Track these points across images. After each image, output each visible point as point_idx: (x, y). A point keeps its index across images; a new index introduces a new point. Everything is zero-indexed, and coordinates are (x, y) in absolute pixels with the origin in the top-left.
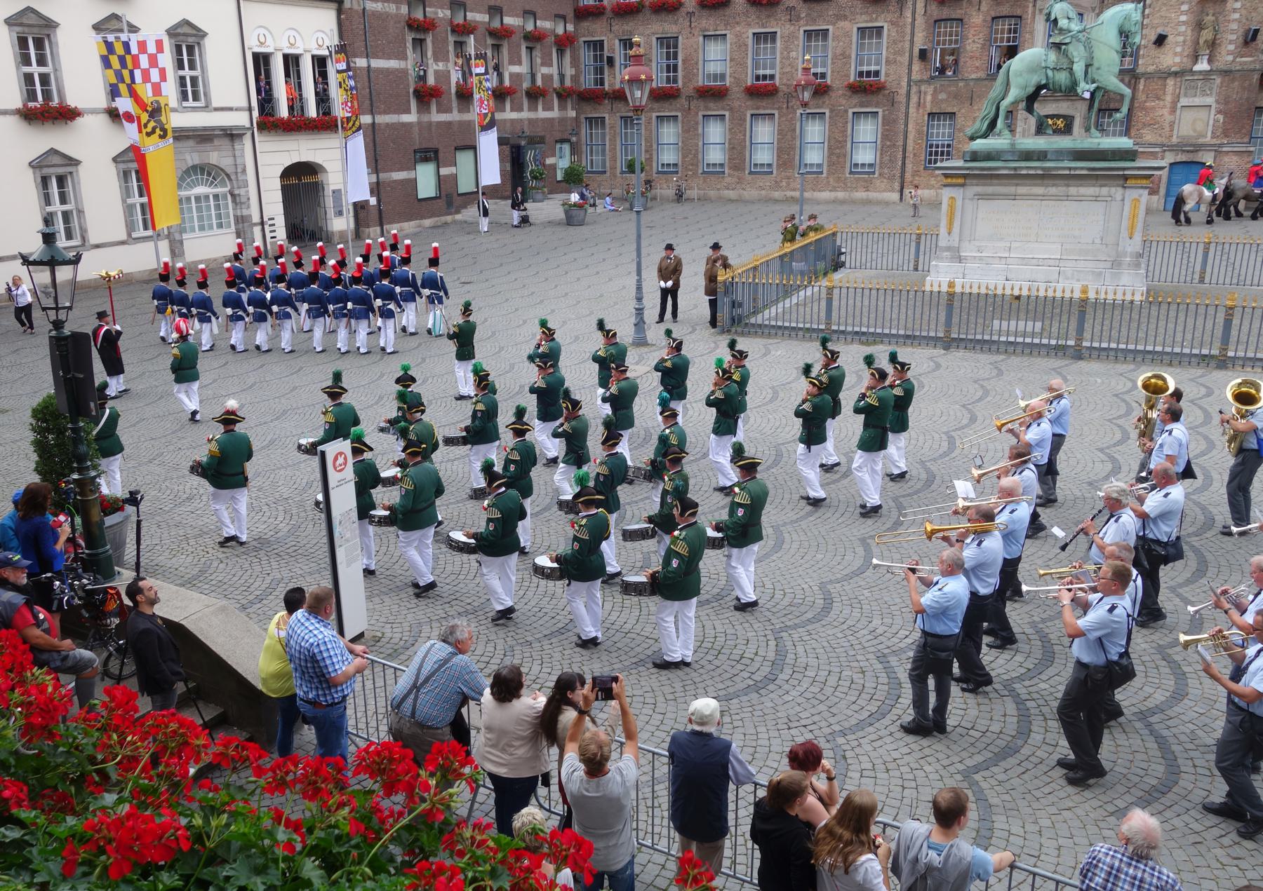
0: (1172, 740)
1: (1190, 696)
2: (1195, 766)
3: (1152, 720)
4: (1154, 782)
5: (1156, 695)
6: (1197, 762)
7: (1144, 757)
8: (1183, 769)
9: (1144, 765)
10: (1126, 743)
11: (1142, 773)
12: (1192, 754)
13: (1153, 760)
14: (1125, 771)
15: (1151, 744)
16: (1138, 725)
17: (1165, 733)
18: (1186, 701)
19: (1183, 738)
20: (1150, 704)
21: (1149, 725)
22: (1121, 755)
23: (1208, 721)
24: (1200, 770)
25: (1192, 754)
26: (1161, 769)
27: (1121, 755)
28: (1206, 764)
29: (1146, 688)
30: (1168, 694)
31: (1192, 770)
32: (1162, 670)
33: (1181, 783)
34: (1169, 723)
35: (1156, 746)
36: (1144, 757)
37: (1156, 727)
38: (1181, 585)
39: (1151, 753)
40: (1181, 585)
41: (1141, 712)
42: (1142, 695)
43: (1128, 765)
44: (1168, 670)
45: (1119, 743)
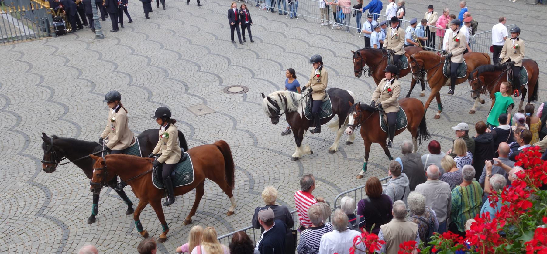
0: (57, 216)
1: (54, 195)
2: (73, 221)
3: (44, 213)
4: (60, 237)
5: (39, 202)
6: (72, 219)
7: (50, 230)
8: (69, 225)
9: (52, 233)
10: (39, 229)
11: (53, 237)
12: (68, 217)
13: (54, 229)
14: (46, 241)
15: (50, 223)
16: (40, 218)
17: (53, 215)
18: (53, 197)
19: (61, 213)
20: (39, 207)
21: (44, 216)
22: (40, 235)
23: (67, 200)
24: (75, 221)
25: (68, 217)
26: (60, 230)
27: (40, 235)
28: (76, 218)
29: (34, 201)
30: (44, 199)
31: (72, 223)
32: (36, 190)
33: (71, 231)
34: (52, 210)
35: (52, 223)
36: (50, 230)
37: (48, 215)
38: (22, 150)
39: (52, 227)
40: (22, 150)
41: (38, 213)
42: (33, 205)
43: (45, 237)
44: (38, 189)
45: (36, 231)
